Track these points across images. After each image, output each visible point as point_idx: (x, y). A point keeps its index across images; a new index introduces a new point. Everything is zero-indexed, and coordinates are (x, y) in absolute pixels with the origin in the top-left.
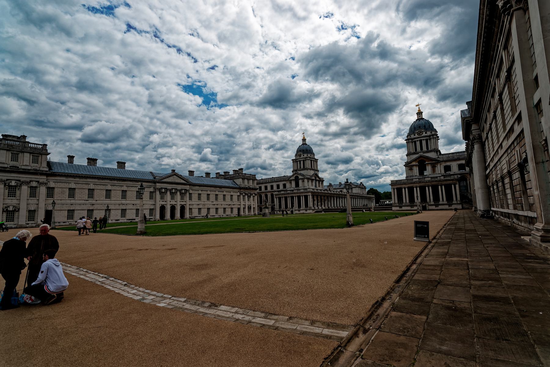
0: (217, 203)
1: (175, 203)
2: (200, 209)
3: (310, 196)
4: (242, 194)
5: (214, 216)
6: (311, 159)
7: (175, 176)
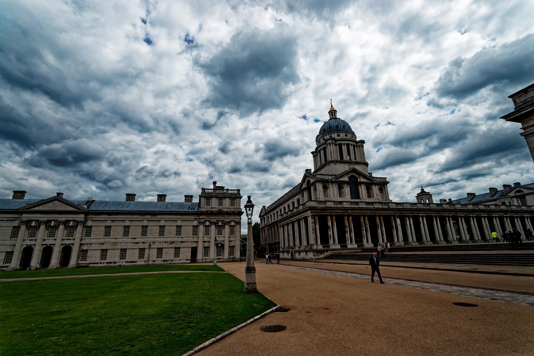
0: (143, 240)
1: (53, 242)
2: (104, 252)
3: (310, 217)
4: (203, 223)
5: (134, 262)
6: (338, 142)
7: (56, 202)
